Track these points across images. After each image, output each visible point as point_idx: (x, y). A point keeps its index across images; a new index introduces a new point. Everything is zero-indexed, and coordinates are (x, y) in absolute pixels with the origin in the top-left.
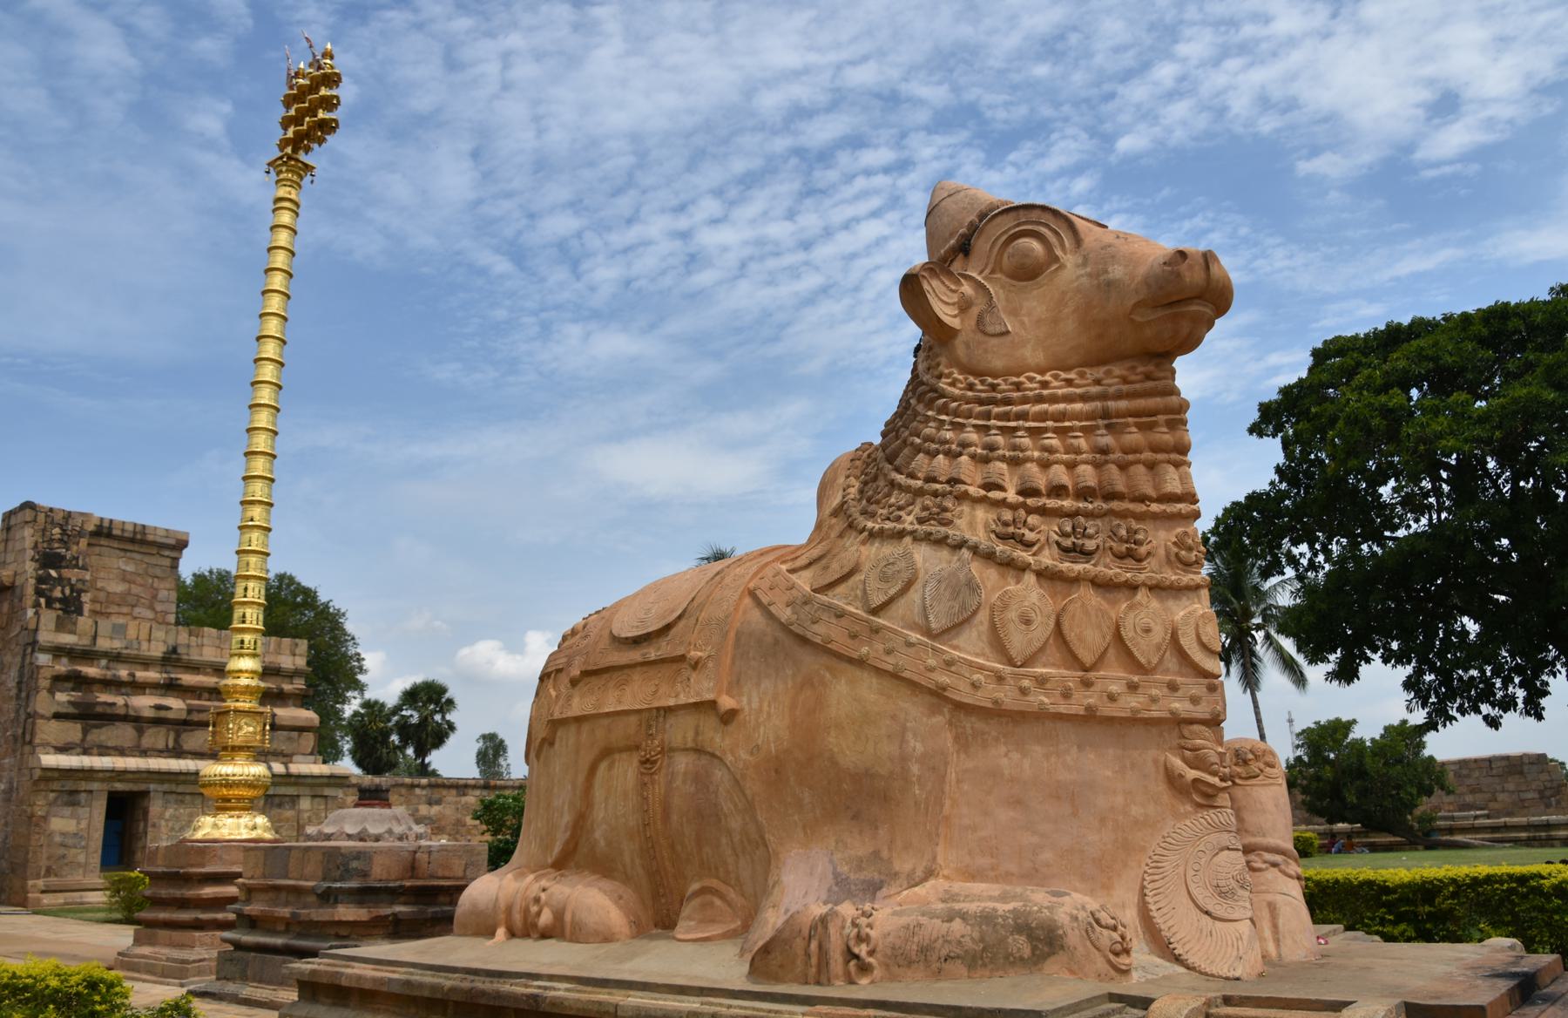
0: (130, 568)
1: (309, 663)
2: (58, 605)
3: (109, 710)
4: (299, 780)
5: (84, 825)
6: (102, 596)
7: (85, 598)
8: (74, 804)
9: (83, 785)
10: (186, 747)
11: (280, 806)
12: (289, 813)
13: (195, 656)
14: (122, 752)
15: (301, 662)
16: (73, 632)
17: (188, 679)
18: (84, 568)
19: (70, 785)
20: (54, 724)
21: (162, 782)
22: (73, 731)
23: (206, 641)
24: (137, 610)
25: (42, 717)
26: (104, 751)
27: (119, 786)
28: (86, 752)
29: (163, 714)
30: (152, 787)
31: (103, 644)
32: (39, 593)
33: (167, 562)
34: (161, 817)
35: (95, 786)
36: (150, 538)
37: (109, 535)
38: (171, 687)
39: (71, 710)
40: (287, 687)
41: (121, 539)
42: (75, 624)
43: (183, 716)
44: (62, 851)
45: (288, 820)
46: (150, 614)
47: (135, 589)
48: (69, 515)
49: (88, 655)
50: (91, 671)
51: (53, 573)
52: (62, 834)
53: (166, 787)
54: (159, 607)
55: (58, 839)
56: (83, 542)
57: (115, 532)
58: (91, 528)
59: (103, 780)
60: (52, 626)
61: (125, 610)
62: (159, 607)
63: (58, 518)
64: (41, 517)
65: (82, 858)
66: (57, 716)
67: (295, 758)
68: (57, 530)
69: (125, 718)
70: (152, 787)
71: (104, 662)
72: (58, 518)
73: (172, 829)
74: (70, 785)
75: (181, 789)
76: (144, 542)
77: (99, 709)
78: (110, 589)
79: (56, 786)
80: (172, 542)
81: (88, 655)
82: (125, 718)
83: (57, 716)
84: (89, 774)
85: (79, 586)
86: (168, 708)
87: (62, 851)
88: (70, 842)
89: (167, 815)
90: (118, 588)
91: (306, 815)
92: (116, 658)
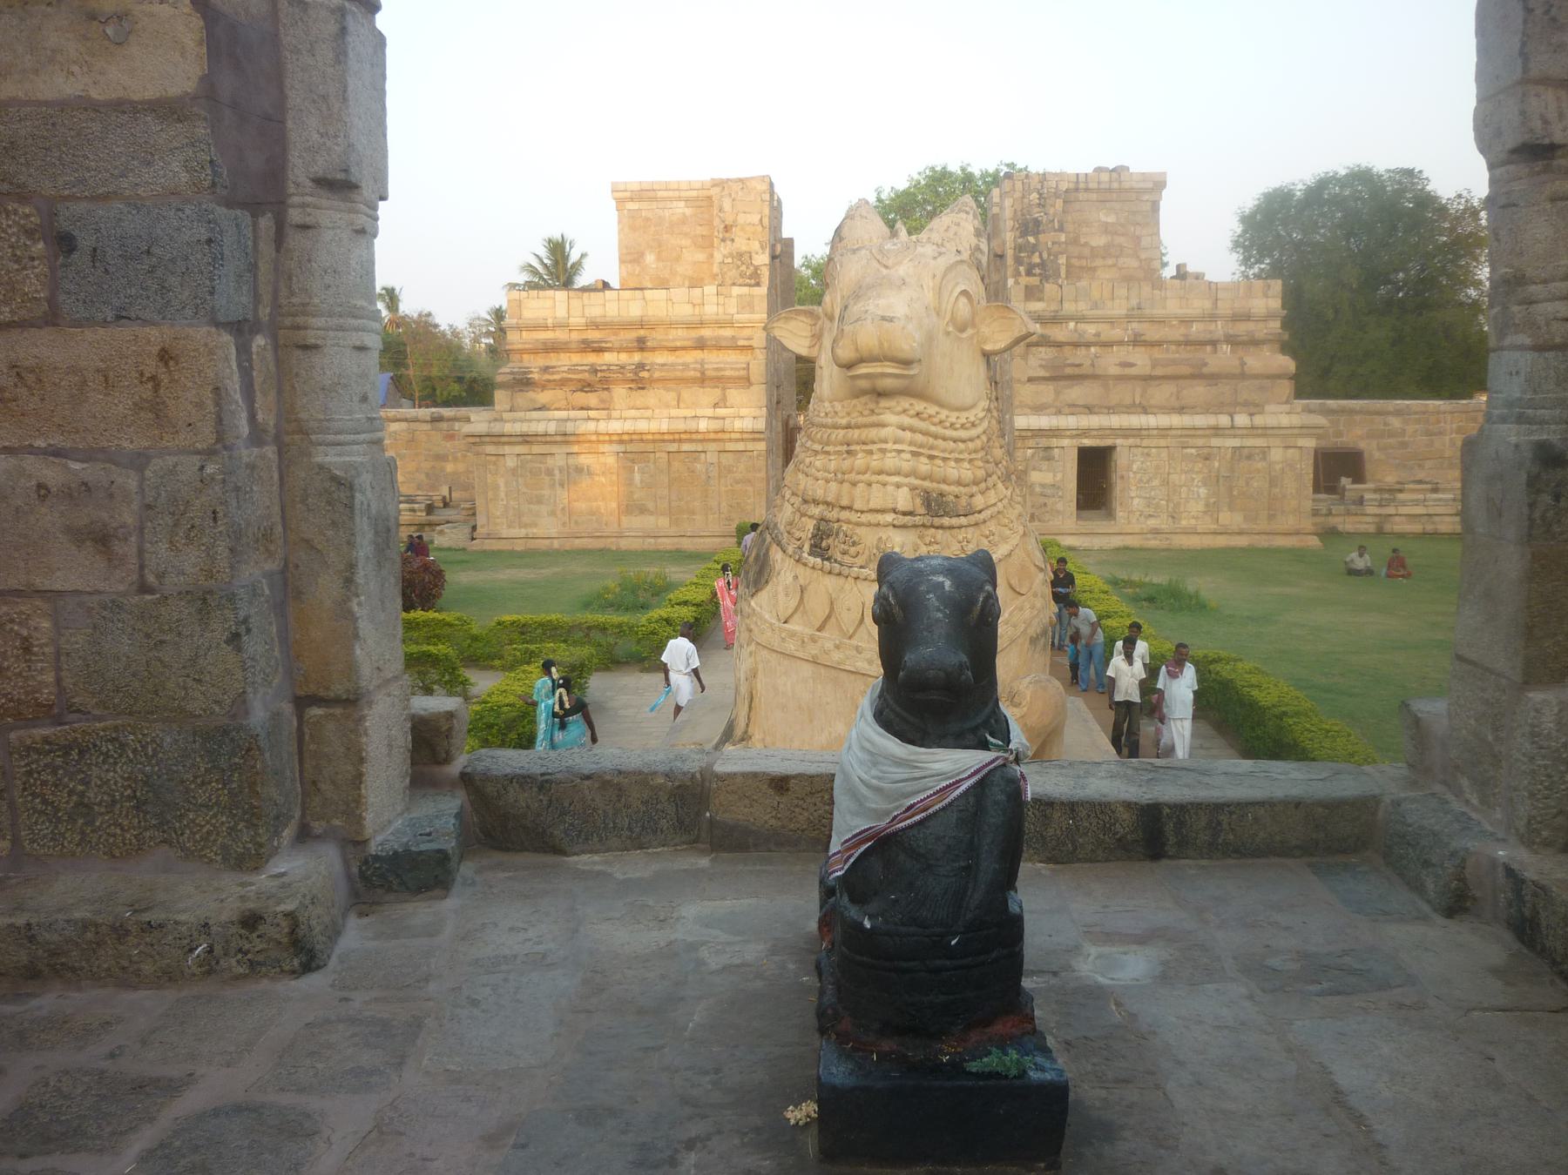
0: (1111, 219)
1: (1283, 307)
2: (1037, 271)
3: (1077, 371)
4: (1265, 431)
5: (1059, 476)
6: (1086, 251)
7: (1062, 260)
8: (1049, 459)
9: (1054, 442)
10: (1153, 402)
11: (1249, 457)
12: (1260, 465)
13: (1158, 312)
14: (1090, 409)
15: (1275, 304)
16: (1040, 300)
17: (1153, 333)
18: (1061, 229)
19: (1044, 442)
20: (1030, 388)
21: (1126, 437)
22: (1047, 392)
23: (1169, 294)
24: (1121, 261)
25: (1019, 381)
26: (1074, 408)
27: (1087, 442)
28: (1059, 412)
29: (1128, 371)
30: (1119, 442)
31: (1069, 308)
32: (1019, 261)
33: (1147, 207)
34: (1129, 468)
35: (1066, 442)
36: (1126, 185)
37: (1087, 190)
38: (1137, 341)
39: (1042, 373)
40: (1260, 335)
41: (1098, 190)
42: (1042, 291)
43: (1147, 371)
44: (1042, 500)
45: (1258, 471)
46: (1135, 263)
47: (1120, 240)
48: (1044, 177)
49: (1056, 319)
50: (1058, 333)
51: (1032, 239)
52: (1043, 486)
53: (1131, 441)
54: (1143, 256)
55: (1038, 489)
56: (1059, 203)
57: (1091, 185)
58: (1064, 186)
59: (1072, 437)
60: (1022, 295)
61: (1110, 262)
62: (1143, 256)
63: (1035, 183)
64: (1019, 185)
65: (1060, 506)
66: (1030, 380)
67: (1269, 408)
68: (1035, 195)
69: (1095, 377)
70: (1119, 442)
71: (1072, 325)
72: (1035, 183)
73: (1141, 481)
74: (1044, 442)
75: (1145, 442)
76: (1121, 190)
77: (1069, 371)
78: (1093, 244)
79: (1031, 443)
80: (1150, 185)
81: (1056, 319)
82: (1095, 377)
83: (1030, 380)
84: (1055, 433)
85: (1056, 248)
86: (1132, 365)
87: (1042, 500)
88: (1049, 491)
89: (1135, 467)
90: (1099, 241)
91: (1278, 467)
92: (1080, 319)
